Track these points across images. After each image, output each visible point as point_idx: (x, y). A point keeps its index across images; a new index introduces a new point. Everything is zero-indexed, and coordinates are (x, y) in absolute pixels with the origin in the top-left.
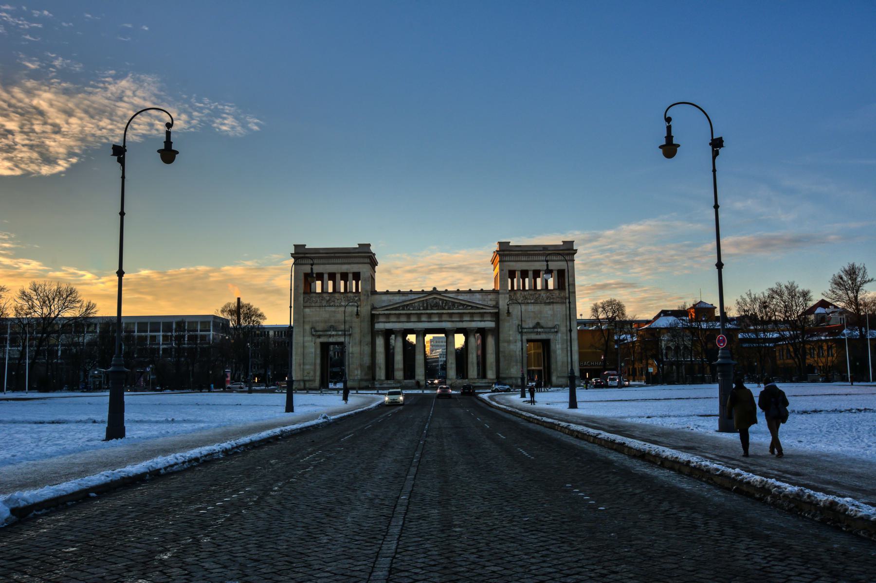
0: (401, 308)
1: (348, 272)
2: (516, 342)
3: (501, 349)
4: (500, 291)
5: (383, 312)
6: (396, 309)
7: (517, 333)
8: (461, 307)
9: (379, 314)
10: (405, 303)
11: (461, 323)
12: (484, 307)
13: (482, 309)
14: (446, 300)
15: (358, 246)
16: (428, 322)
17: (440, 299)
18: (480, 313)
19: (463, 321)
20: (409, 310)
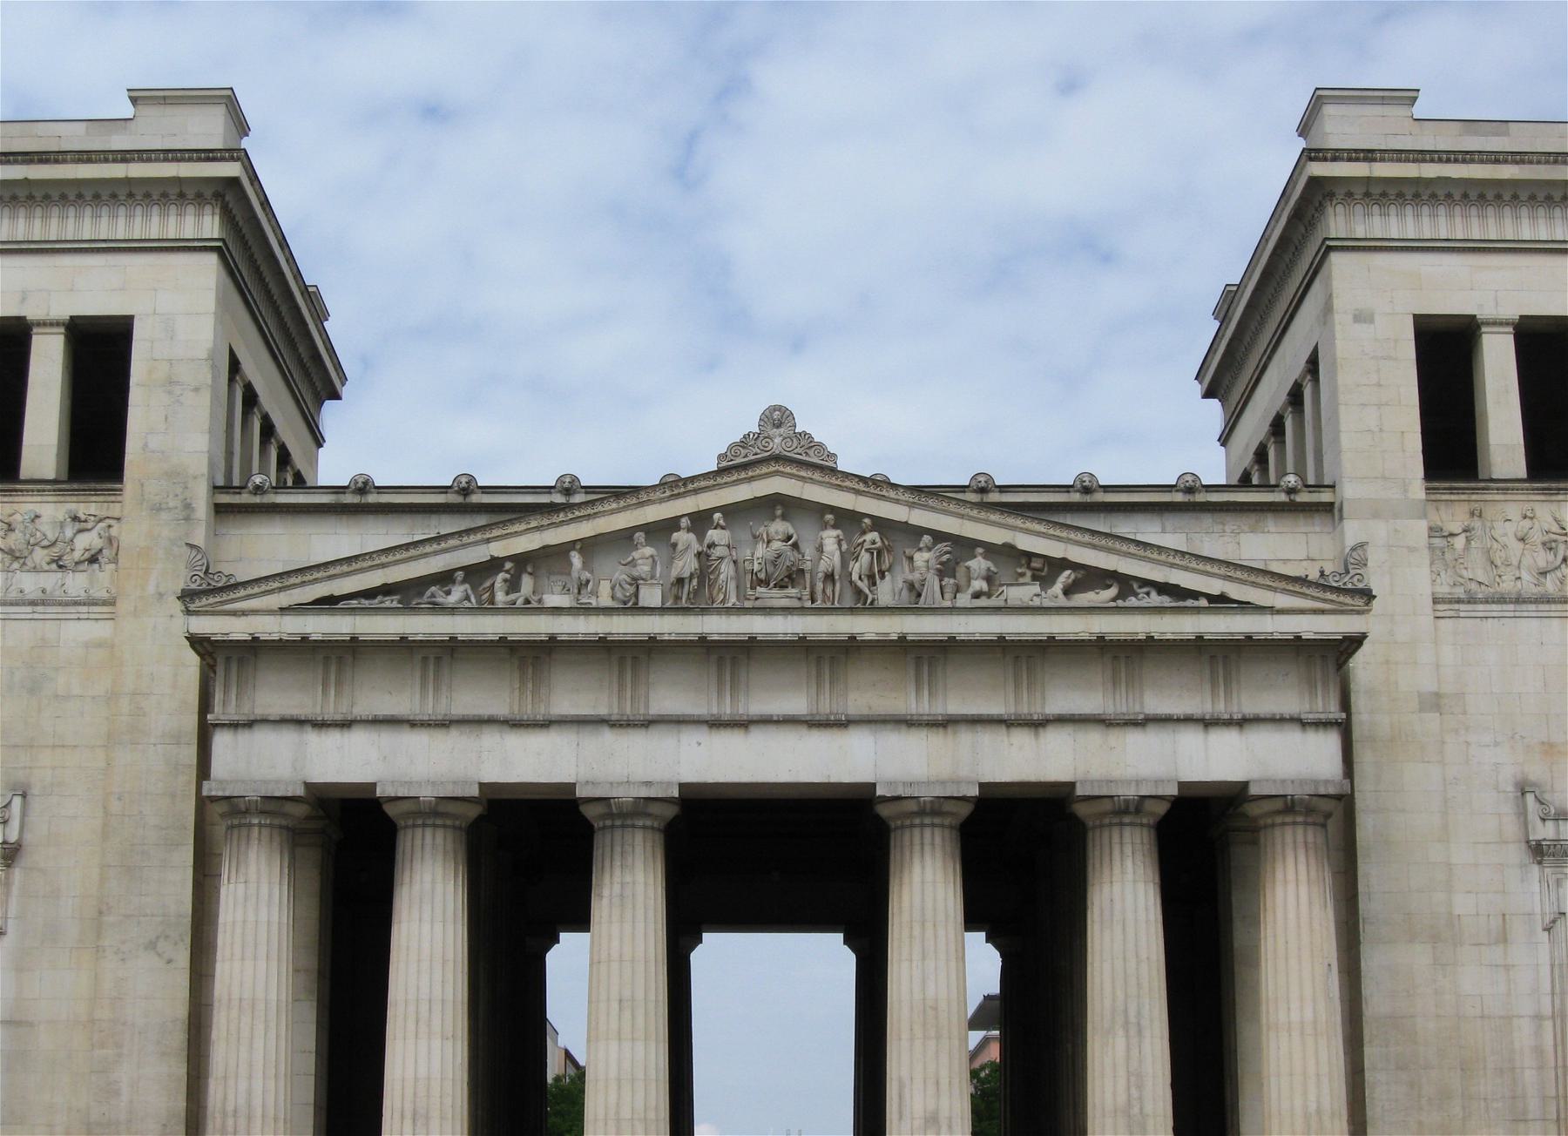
0: (457, 593)
1: (31, 312)
2: (1503, 938)
3: (1375, 1003)
4: (1350, 491)
5: (294, 626)
6: (408, 594)
7: (1516, 854)
8: (1024, 593)
9: (254, 649)
10: (499, 549)
11: (1021, 739)
12: (1235, 591)
13: (1220, 602)
14: (880, 524)
15: (127, 110)
16: (716, 724)
17: (847, 520)
18: (1200, 649)
19: (1037, 724)
20: (530, 608)
